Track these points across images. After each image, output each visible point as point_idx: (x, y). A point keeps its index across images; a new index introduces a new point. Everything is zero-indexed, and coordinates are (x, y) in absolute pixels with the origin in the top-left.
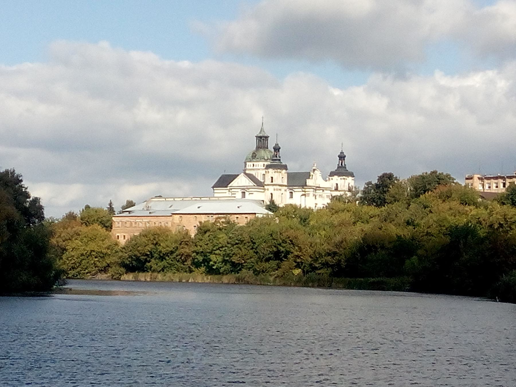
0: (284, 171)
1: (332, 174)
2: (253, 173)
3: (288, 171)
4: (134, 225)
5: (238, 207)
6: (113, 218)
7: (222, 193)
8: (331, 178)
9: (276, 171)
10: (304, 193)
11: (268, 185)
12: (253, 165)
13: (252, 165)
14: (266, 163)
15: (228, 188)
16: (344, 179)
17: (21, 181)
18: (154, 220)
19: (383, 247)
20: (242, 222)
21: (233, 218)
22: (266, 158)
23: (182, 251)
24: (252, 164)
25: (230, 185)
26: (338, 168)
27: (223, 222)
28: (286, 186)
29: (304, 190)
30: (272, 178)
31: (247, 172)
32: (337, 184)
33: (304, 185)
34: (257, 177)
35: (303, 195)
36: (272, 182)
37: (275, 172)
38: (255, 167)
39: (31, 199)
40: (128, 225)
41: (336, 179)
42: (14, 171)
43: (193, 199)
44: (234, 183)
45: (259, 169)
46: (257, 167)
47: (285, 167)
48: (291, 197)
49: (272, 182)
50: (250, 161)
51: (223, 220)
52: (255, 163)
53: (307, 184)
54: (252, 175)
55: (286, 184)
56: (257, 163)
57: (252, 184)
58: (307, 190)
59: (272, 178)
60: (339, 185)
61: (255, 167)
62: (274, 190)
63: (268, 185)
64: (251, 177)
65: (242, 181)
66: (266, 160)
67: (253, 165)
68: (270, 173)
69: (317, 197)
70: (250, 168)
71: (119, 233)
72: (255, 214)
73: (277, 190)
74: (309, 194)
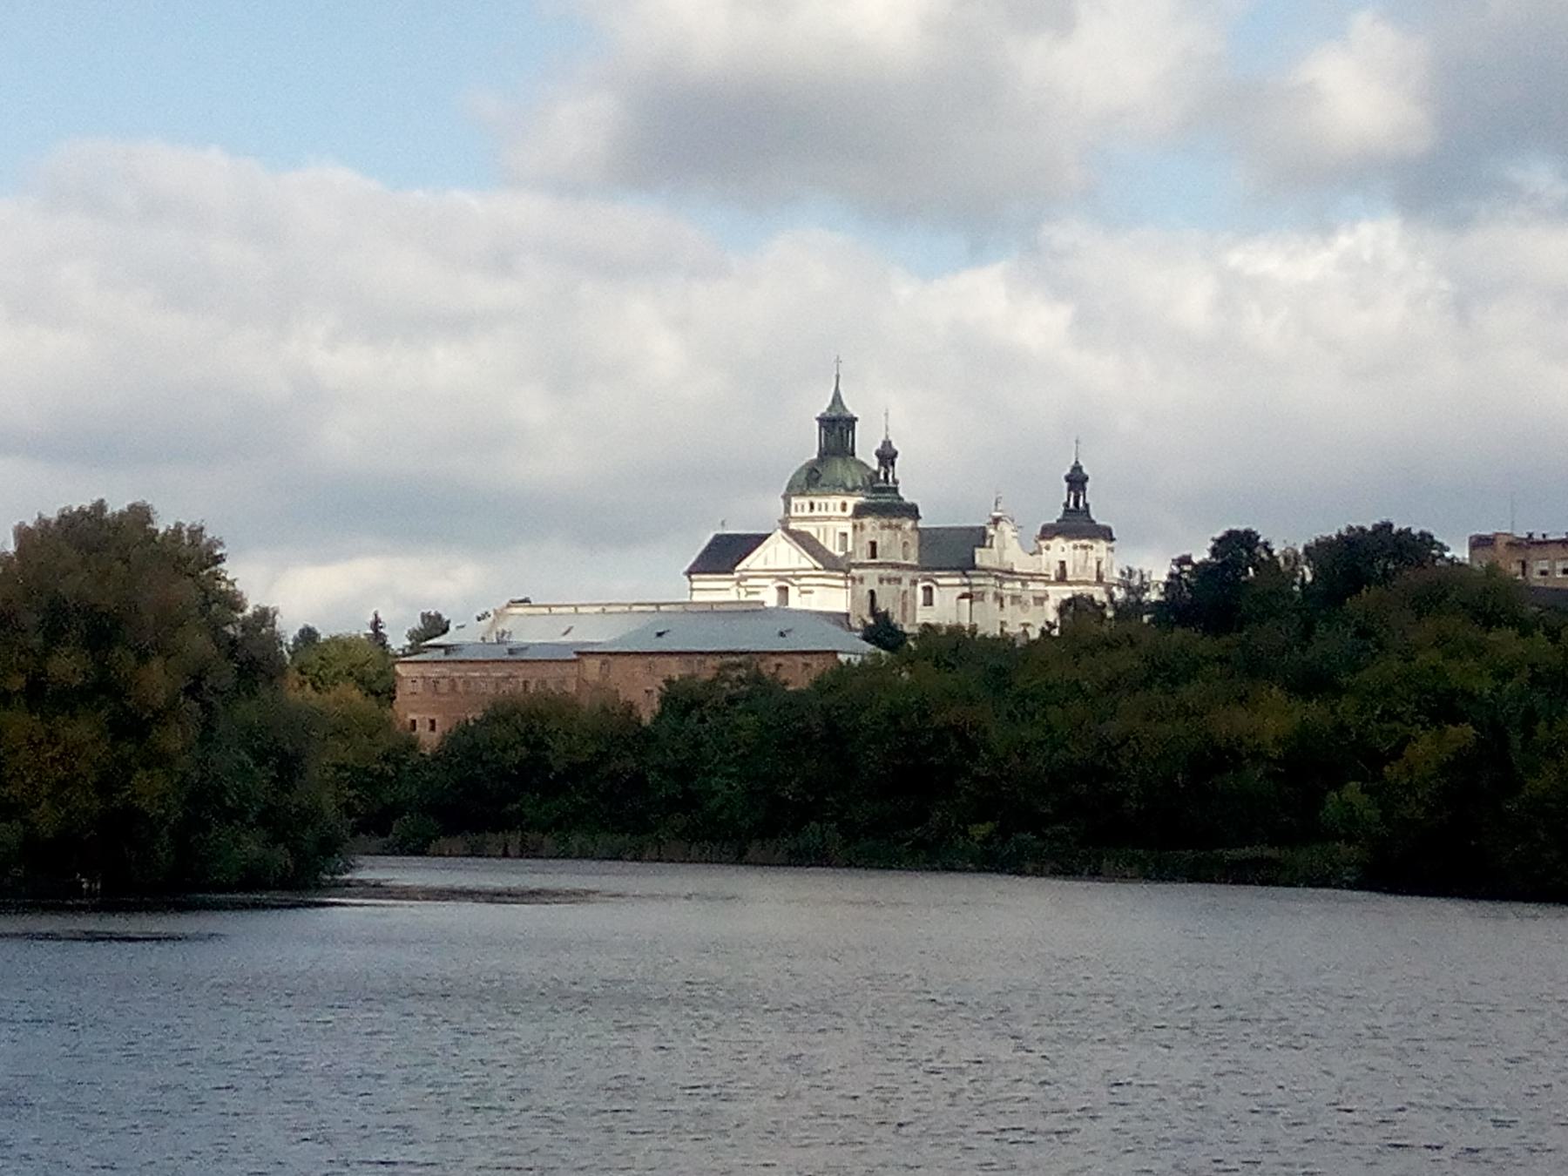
0: (909, 524)
1: (1048, 532)
2: (810, 528)
3: (920, 525)
4: (460, 688)
5: (782, 634)
6: (398, 667)
7: (717, 590)
8: (1043, 543)
9: (885, 521)
10: (966, 590)
13: (807, 507)
14: (851, 502)
15: (736, 575)
16: (1085, 547)
17: (219, 559)
18: (522, 673)
19: (1257, 755)
20: (798, 679)
21: (768, 667)
22: (849, 484)
23: (616, 765)
24: (806, 501)
25: (739, 568)
26: (1067, 511)
27: (739, 679)
28: (912, 568)
29: (966, 580)
31: (793, 526)
32: (1063, 563)
33: (966, 566)
34: (821, 541)
35: (963, 596)
36: (874, 556)
37: (883, 527)
38: (816, 513)
39: (249, 612)
40: (444, 686)
42: (202, 529)
43: (635, 608)
44: (754, 561)
45: (829, 518)
46: (823, 513)
47: (912, 512)
48: (929, 602)
49: (874, 556)
50: (802, 494)
51: (743, 673)
52: (817, 501)
53: (977, 561)
54: (808, 535)
55: (913, 561)
56: (823, 500)
57: (808, 562)
58: (975, 581)
59: (873, 544)
60: (1069, 567)
61: (816, 513)
62: (881, 581)
64: (805, 541)
65: (778, 553)
66: (850, 491)
68: (869, 529)
69: (1007, 601)
70: (800, 514)
71: (414, 711)
72: (835, 652)
73: (889, 580)
74: (983, 594)
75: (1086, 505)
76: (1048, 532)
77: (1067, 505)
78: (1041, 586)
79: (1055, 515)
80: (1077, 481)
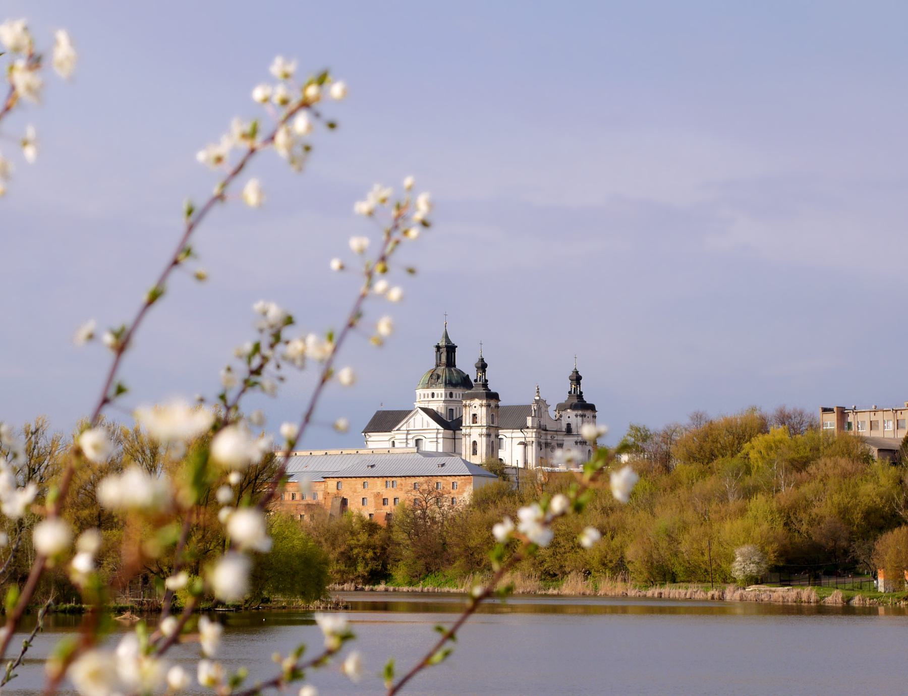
10: (523, 440)
11: (471, 427)
12: (433, 395)
13: (430, 396)
15: (393, 433)
24: (430, 391)
29: (521, 435)
30: (474, 415)
33: (523, 427)
35: (521, 443)
41: (571, 417)
44: (403, 426)
52: (436, 391)
57: (434, 425)
63: (471, 427)
67: (433, 395)
75: (581, 393)
76: (561, 408)
77: (570, 393)
78: (559, 438)
79: (564, 398)
80: (577, 379)
